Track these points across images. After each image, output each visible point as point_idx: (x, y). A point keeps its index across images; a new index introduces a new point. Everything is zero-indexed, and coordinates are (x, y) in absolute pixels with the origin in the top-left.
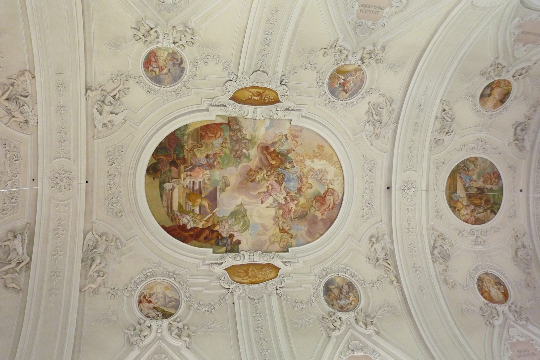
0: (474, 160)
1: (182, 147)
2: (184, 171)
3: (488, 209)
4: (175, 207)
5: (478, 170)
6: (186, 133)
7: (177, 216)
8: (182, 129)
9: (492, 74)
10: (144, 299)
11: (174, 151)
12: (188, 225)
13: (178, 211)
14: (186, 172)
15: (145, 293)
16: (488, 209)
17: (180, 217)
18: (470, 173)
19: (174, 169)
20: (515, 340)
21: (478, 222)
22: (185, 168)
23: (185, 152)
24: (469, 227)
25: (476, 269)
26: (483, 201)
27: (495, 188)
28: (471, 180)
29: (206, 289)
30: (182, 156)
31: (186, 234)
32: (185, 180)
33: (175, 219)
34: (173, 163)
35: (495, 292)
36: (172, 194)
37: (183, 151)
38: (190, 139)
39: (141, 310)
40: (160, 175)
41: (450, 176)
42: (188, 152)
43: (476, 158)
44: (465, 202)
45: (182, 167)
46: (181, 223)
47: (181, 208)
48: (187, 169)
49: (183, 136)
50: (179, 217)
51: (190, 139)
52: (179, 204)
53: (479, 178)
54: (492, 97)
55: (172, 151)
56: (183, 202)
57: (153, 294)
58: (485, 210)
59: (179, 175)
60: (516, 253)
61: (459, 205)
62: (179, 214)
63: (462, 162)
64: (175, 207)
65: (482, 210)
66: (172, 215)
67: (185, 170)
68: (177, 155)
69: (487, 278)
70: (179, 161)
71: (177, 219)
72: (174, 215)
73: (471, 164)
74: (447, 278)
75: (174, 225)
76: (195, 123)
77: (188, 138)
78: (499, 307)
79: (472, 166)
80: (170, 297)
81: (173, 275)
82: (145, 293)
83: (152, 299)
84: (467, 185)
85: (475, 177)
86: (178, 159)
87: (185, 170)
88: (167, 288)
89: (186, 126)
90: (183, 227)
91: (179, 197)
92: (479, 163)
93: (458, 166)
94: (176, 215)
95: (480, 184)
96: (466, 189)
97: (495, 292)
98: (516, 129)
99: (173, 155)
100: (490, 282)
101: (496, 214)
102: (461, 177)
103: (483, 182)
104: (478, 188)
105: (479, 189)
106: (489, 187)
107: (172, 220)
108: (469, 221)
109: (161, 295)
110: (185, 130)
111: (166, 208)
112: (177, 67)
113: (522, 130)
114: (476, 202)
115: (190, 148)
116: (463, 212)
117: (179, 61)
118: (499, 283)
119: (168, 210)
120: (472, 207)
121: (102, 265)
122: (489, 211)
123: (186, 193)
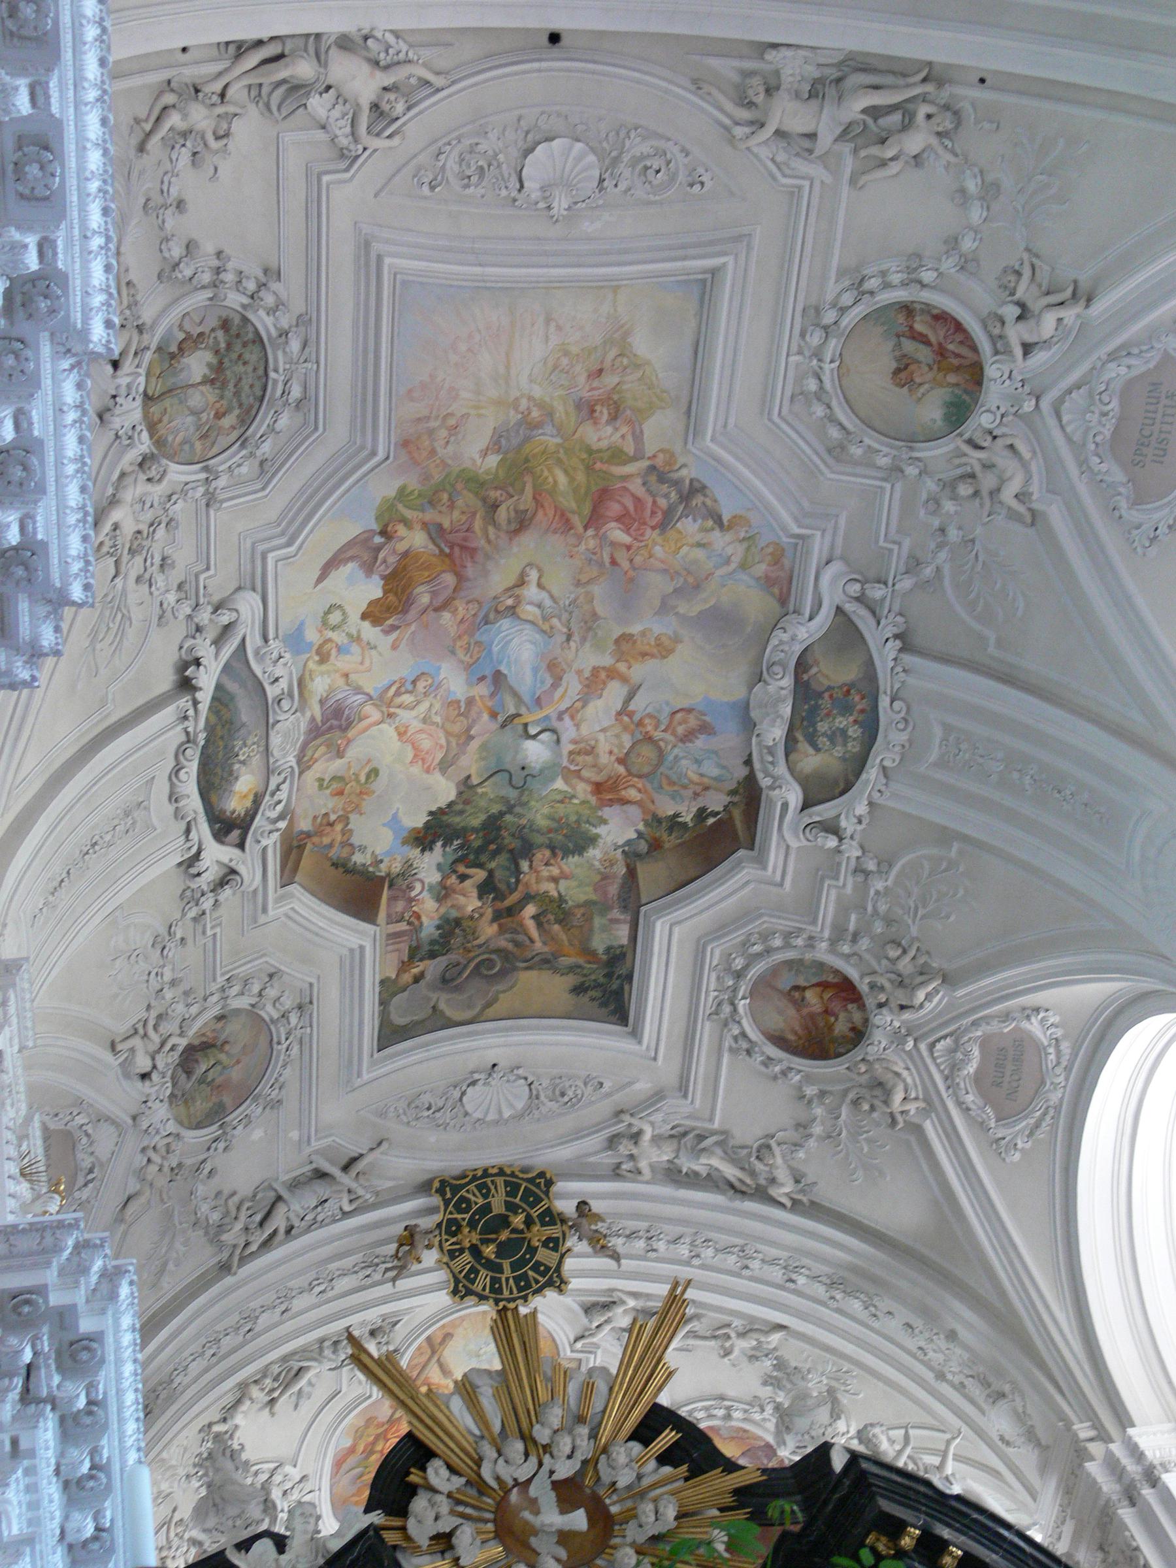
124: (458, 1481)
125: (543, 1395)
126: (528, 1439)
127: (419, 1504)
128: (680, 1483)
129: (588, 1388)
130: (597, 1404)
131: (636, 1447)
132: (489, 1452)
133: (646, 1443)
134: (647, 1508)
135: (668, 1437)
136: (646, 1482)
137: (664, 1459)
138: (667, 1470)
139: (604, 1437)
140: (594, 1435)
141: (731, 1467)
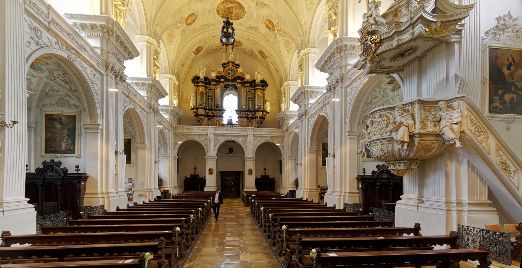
0: (244, 11)
3: (224, 15)
5: (240, 12)
9: (277, 27)
16: (224, 15)
18: (239, 10)
20: (174, 32)
21: (218, 11)
24: (216, 8)
25: (198, 12)
26: (227, 13)
27: (232, 18)
28: (236, 9)
35: (190, 21)
41: (237, 2)
43: (245, 12)
44: (226, 7)
53: (237, 12)
54: (269, 23)
58: (223, 14)
60: (206, 25)
61: (225, 4)
63: (243, 7)
65: (223, 13)
69: (195, 16)
73: (243, 10)
74: (192, 2)
78: (184, 24)
79: (242, 10)
84: (233, 8)
85: (237, 11)
92: (243, 13)
93: (242, 5)
95: (234, 12)
96: (232, 7)
97: (190, 21)
98: (256, 28)
100: (193, 18)
101: (222, 17)
102: (237, 6)
103: (235, 14)
104: (232, 11)
105: (232, 12)
106: (233, 15)
108: (218, 8)
113: (256, 30)
114: (226, 11)
116: (222, 6)
118: (194, 21)
120: (224, 9)
122: (223, 15)
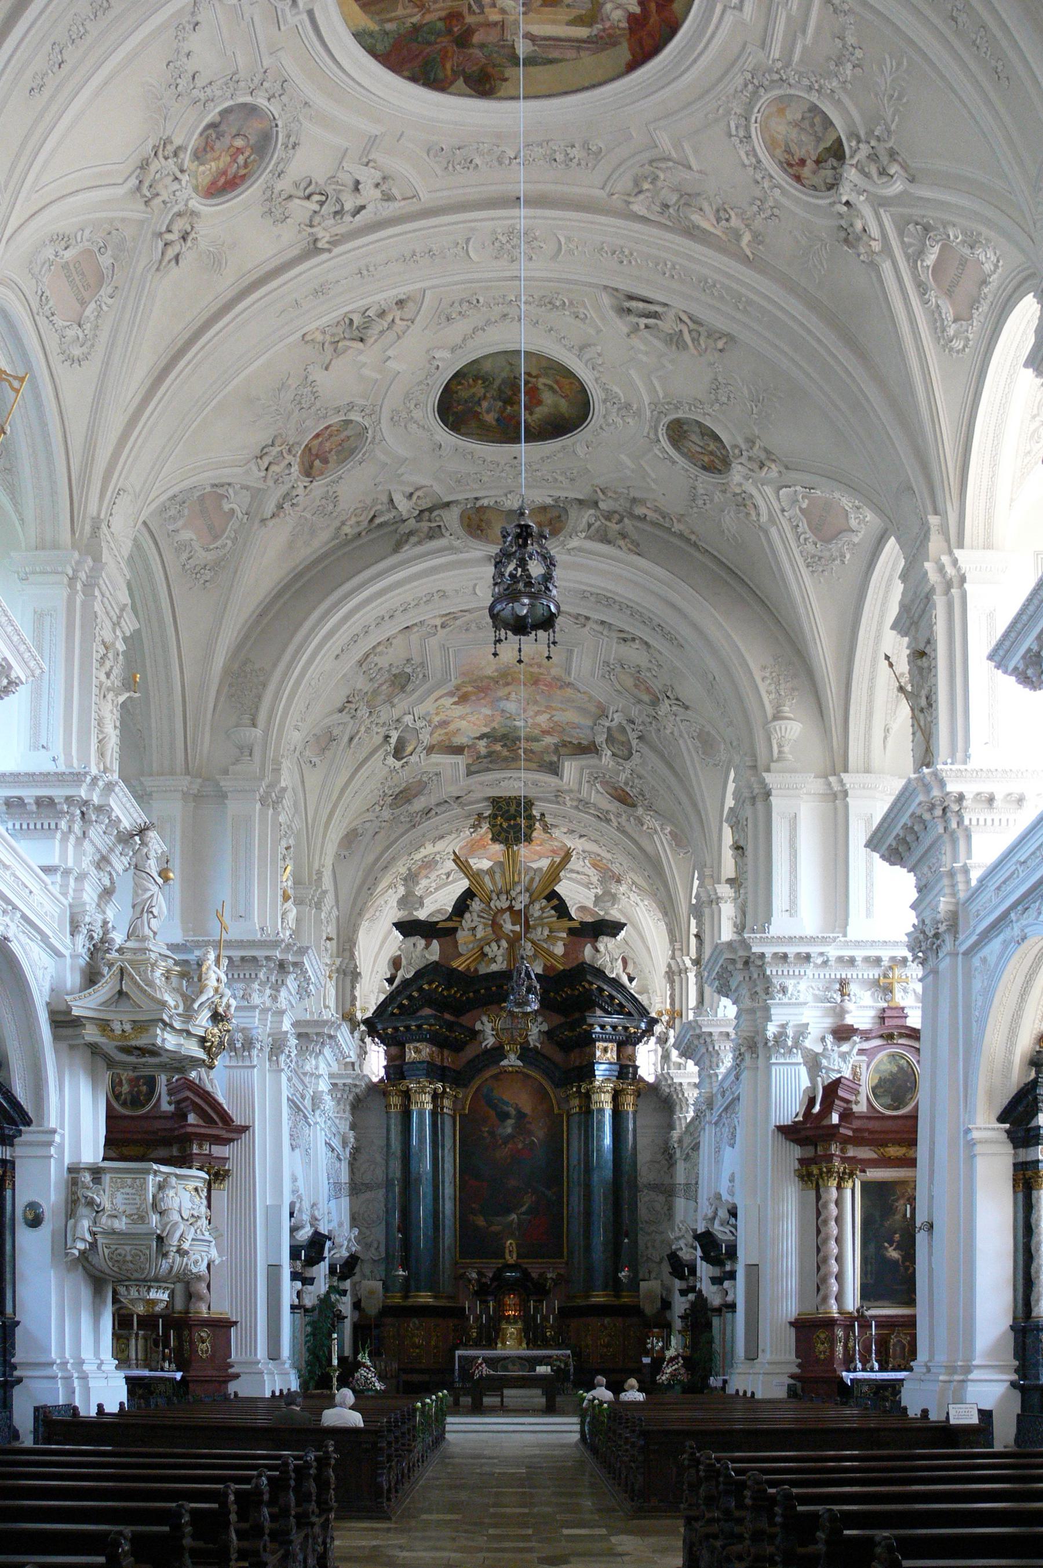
1: (416, 28)
2: (482, 12)
4: (582, 32)
6: (377, 28)
7: (604, 30)
8: (370, 41)
10: (794, 167)
11: (429, 44)
12: (631, 11)
13: (591, 25)
14: (486, 10)
15: (783, 160)
17: (608, 25)
19: (476, 38)
22: (474, 13)
23: (428, 18)
29: (804, 32)
30: (440, 25)
31: (654, 19)
32: (507, 9)
33: (610, 36)
34: (463, 40)
36: (545, 39)
37: (426, 24)
38: (393, 14)
39: (815, 188)
40: (494, 66)
42: (429, 11)
45: (470, 19)
46: (624, 25)
47: (582, 20)
48: (475, 7)
49: (386, 33)
50: (607, 27)
51: (393, 14)
52: (570, 23)
55: (428, 50)
56: (563, 14)
57: (787, 145)
59: (496, 24)
62: (600, 26)
64: (582, 32)
66: (602, 43)
67: (477, 11)
68: (439, 34)
70: (456, 29)
71: (610, 31)
72: (602, 38)
75: (629, 40)
76: (346, 18)
77: (390, 20)
80: (803, 118)
81: (755, 86)
82: (783, 160)
83: (799, 153)
86: (449, 31)
87: (477, 11)
88: (781, 111)
89: (358, 36)
90: (636, 22)
91: (554, 22)
94: (602, 34)
99: (438, 47)
107: (614, 44)
109: (794, 134)
110: (371, 35)
111: (582, 54)
112: (223, 127)
115: (417, 10)
117: (210, 131)
119: (588, 49)
121: (706, 206)
123: (542, 6)
124: (483, 906)
125: (516, 879)
126: (508, 892)
127: (467, 915)
128: (555, 919)
129: (532, 880)
130: (535, 885)
131: (544, 902)
132: (494, 896)
133: (549, 901)
134: (539, 929)
135: (555, 902)
136: (545, 915)
137: (552, 908)
138: (553, 912)
139: (533, 898)
140: (530, 896)
141: (571, 919)
